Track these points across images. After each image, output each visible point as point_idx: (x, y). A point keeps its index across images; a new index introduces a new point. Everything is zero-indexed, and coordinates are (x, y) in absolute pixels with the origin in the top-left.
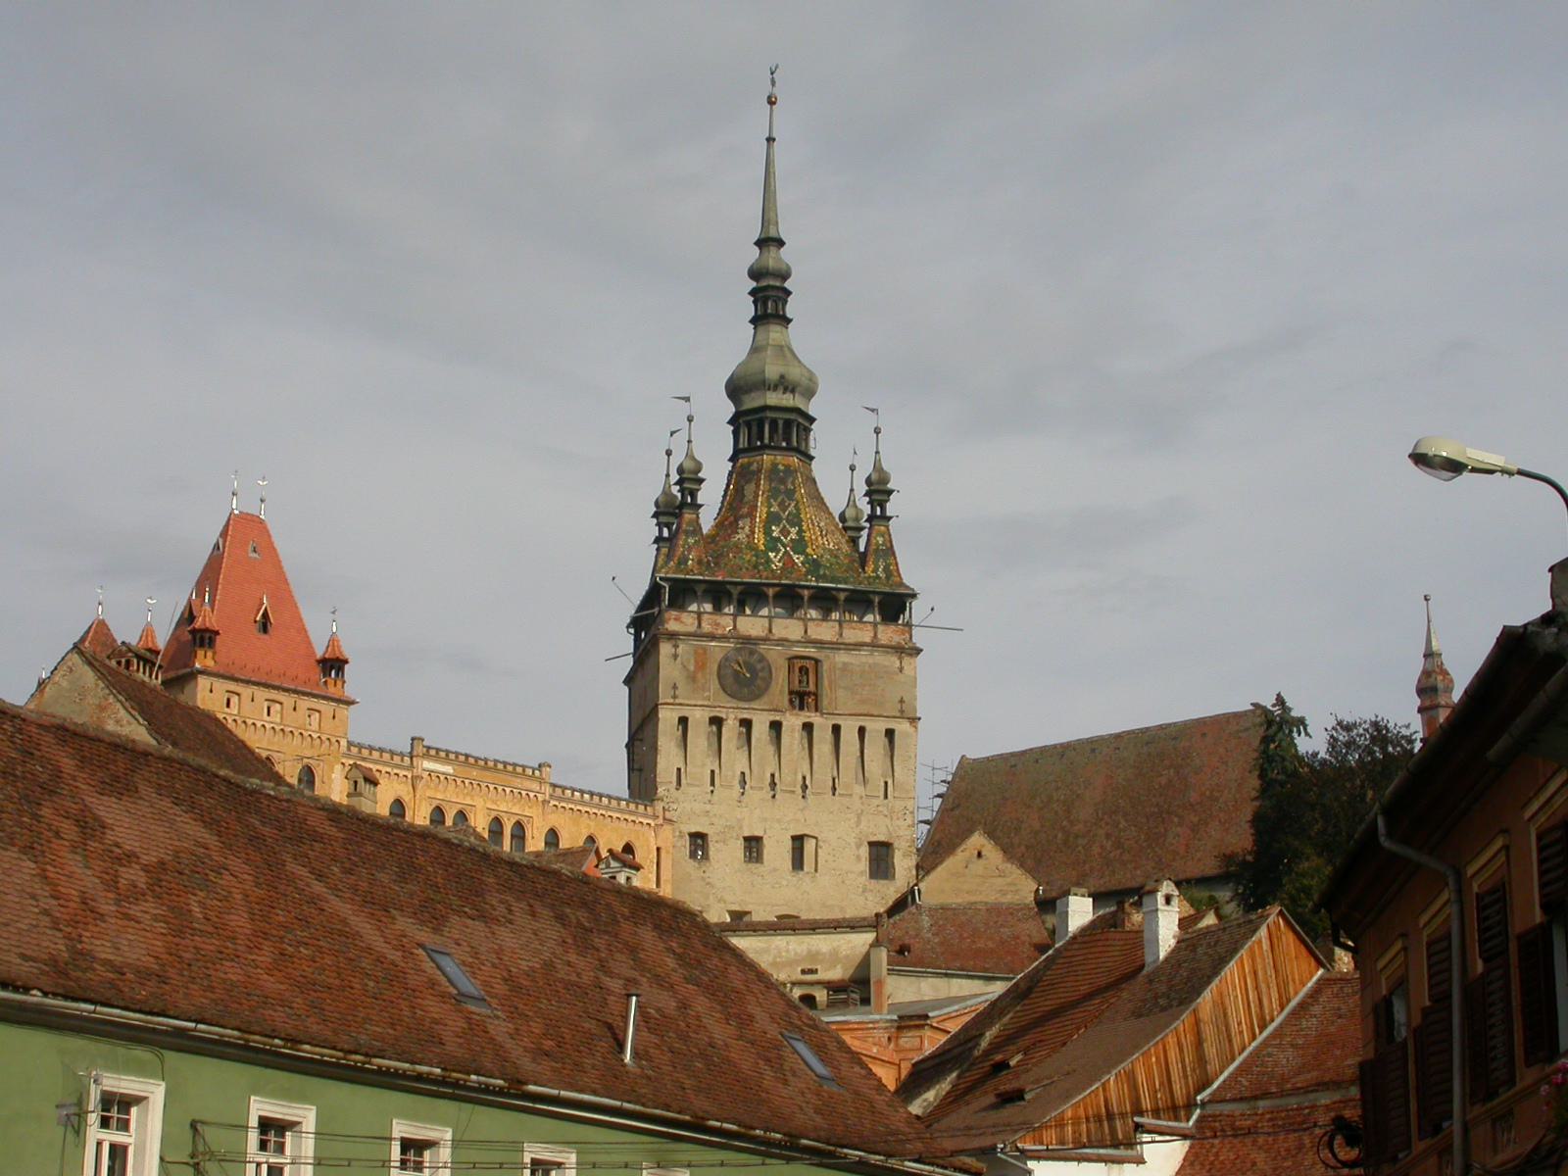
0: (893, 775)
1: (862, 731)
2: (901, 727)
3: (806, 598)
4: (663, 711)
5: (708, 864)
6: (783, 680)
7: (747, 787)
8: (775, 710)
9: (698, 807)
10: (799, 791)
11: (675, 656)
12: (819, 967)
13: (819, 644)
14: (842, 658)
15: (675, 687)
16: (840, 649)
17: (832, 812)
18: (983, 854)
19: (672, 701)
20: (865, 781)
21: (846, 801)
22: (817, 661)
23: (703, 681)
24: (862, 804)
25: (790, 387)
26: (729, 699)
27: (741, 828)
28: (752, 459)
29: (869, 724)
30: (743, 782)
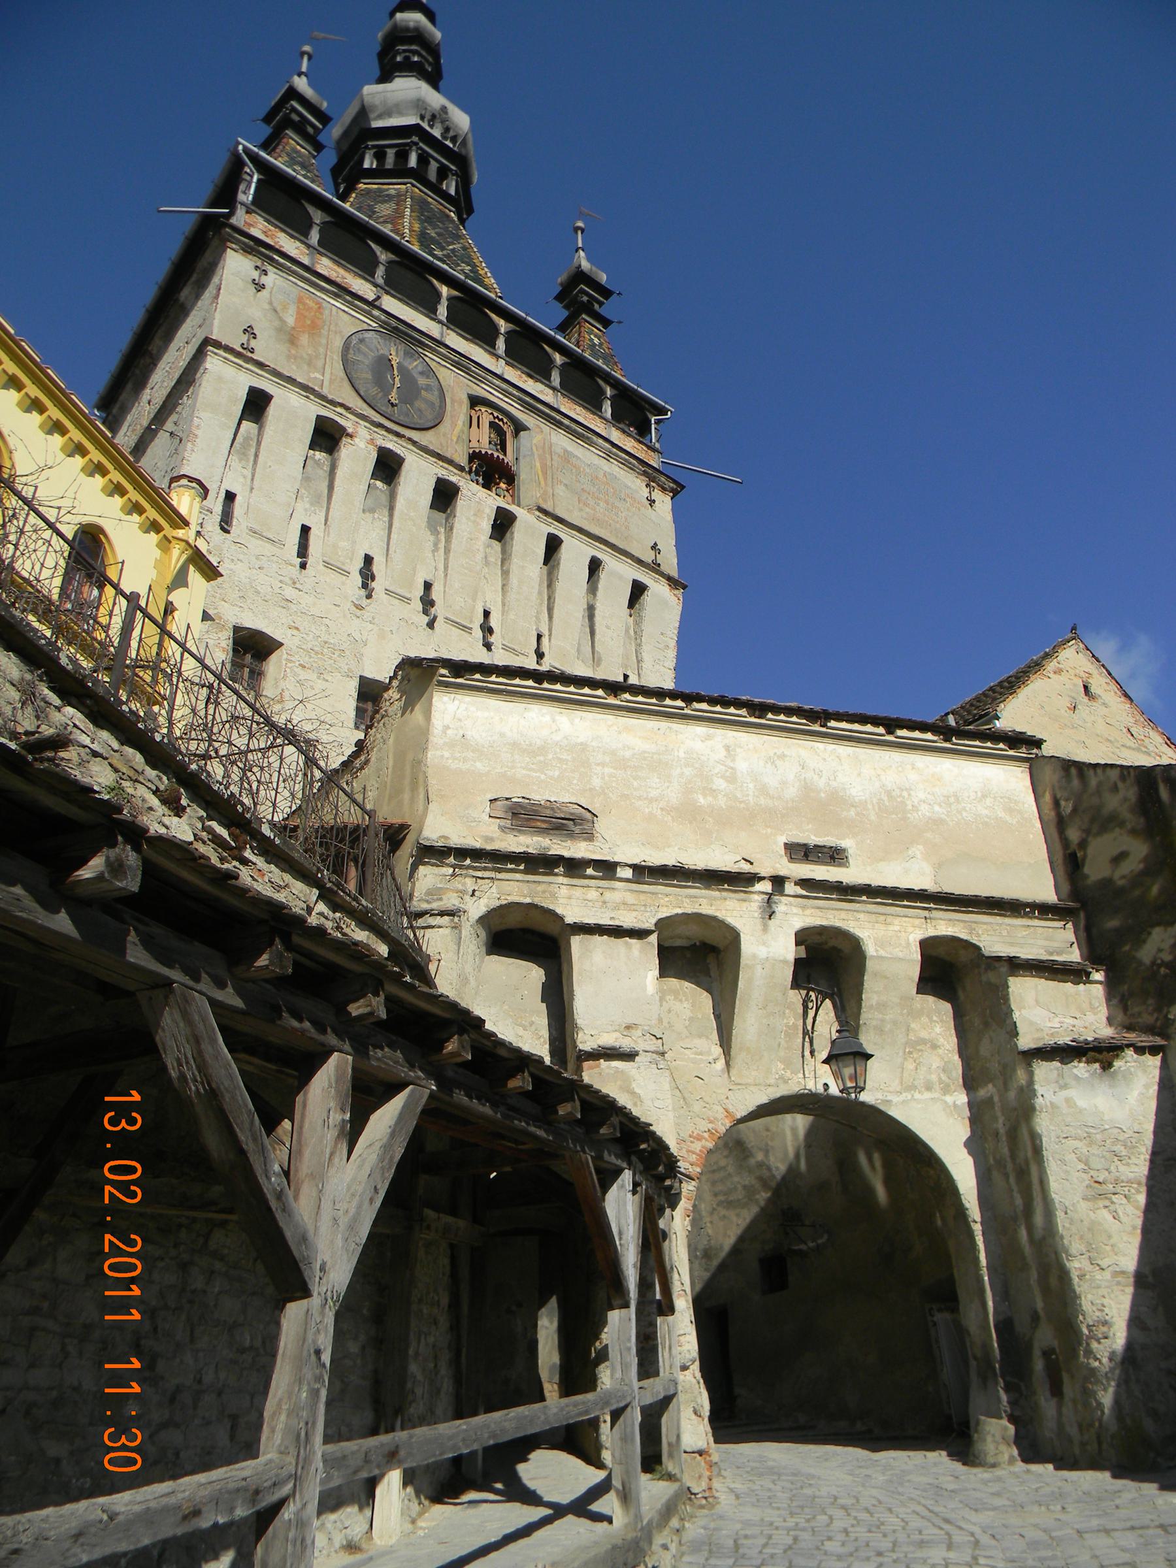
1: (595, 566)
2: (658, 589)
4: (214, 361)
6: (464, 425)
7: (377, 585)
8: (450, 462)
10: (479, 634)
11: (259, 287)
13: (531, 403)
14: (561, 440)
15: (249, 331)
16: (559, 424)
18: (1093, 689)
19: (241, 350)
22: (519, 428)
25: (451, 134)
27: (359, 658)
29: (610, 562)
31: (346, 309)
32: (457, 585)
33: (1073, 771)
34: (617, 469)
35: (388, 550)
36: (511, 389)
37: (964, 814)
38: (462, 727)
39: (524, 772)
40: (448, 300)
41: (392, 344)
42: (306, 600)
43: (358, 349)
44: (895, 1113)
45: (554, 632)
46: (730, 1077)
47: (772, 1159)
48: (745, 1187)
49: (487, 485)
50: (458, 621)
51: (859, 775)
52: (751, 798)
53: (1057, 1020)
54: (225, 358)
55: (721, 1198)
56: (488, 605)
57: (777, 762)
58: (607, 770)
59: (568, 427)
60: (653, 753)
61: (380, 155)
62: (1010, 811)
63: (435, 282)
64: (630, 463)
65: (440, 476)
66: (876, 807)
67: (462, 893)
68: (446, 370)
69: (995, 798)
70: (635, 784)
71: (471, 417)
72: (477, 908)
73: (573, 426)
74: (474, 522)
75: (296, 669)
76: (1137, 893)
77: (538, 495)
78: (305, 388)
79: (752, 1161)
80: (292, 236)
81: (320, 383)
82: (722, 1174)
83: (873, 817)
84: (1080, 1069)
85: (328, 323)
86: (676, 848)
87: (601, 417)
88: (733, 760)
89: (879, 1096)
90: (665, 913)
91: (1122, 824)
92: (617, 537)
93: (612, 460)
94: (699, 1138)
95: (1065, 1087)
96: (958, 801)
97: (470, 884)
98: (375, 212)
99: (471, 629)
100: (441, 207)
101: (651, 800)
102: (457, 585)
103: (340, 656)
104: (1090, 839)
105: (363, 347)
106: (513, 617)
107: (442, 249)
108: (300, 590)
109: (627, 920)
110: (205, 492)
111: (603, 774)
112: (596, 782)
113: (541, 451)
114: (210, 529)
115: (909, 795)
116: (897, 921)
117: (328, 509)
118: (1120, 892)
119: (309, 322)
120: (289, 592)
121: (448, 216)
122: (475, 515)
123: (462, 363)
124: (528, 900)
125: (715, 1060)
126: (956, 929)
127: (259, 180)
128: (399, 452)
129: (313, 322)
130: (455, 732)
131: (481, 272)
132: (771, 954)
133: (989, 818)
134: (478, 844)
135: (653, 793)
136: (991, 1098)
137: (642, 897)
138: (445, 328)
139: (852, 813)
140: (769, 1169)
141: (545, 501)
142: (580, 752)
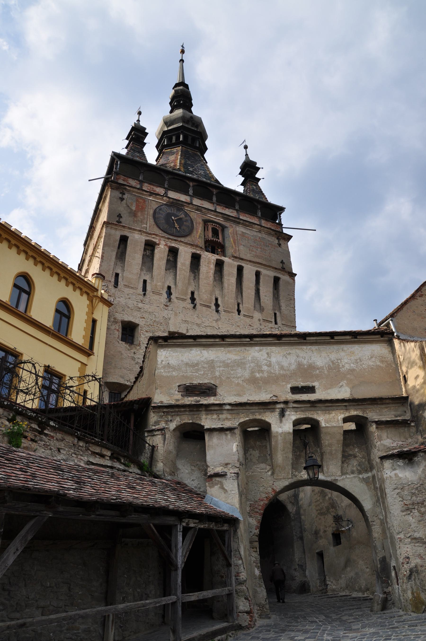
0: (280, 309)
2: (284, 278)
3: (215, 193)
5: (138, 348)
6: (201, 231)
7: (172, 296)
8: (197, 246)
9: (131, 303)
10: (214, 307)
11: (122, 199)
12: (316, 384)
13: (227, 218)
14: (240, 229)
15: (120, 216)
16: (239, 223)
17: (238, 326)
19: (117, 223)
20: (261, 310)
21: (248, 320)
22: (223, 228)
23: (141, 218)
24: (261, 324)
26: (161, 232)
27: (167, 324)
28: (173, 149)
29: (264, 272)
30: (169, 293)
31: (154, 200)
32: (203, 291)
33: (402, 344)
34: (264, 235)
35: (176, 283)
36: (218, 215)
37: (363, 366)
38: (168, 360)
39: (191, 374)
40: (192, 187)
41: (172, 208)
42: (147, 307)
43: (159, 213)
44: (340, 484)
45: (244, 302)
46: (274, 477)
47: (333, 497)
48: (325, 507)
49: (213, 252)
50: (205, 304)
51: (320, 356)
52: (277, 372)
53: (396, 443)
54: (111, 227)
55: (319, 512)
56: (217, 296)
57: (288, 356)
58: (221, 369)
59: (243, 223)
60: (239, 360)
61: (170, 139)
62: (382, 361)
63: (187, 182)
64: (269, 232)
65: (193, 252)
66: (327, 368)
67: (167, 422)
68: (193, 213)
69: (376, 357)
70: (232, 372)
71: (204, 227)
72: (173, 426)
73: (244, 222)
74: (208, 266)
75: (144, 333)
76: (422, 391)
77: (233, 251)
78: (140, 231)
79: (327, 498)
80: (133, 179)
81: (146, 228)
82: (318, 503)
83: (326, 372)
84: (400, 463)
85: (147, 206)
86: (248, 395)
87: (256, 217)
88: (270, 358)
89: (333, 478)
90: (242, 420)
91: (416, 364)
92: (266, 261)
93: (262, 232)
94: (262, 500)
95: (395, 469)
96: (361, 361)
97: (170, 418)
98: (168, 159)
99: (210, 306)
100: (193, 151)
101: (238, 378)
102: (203, 291)
103: (160, 325)
104: (408, 370)
105: (161, 212)
106: (227, 299)
107: (193, 167)
108: (144, 304)
109: (228, 424)
110: (104, 277)
111: (220, 370)
112: (217, 374)
113: (232, 235)
114: (110, 288)
115: (341, 361)
116: (333, 412)
117: (152, 272)
118: (418, 391)
119: (140, 207)
120: (140, 305)
121: (196, 154)
122: (208, 264)
123: (199, 209)
124: (191, 421)
125: (268, 471)
126: (358, 412)
127: (120, 163)
128: (176, 246)
129: (142, 207)
130: (165, 362)
131: (208, 172)
132: (283, 431)
133: (373, 365)
134: (173, 402)
135: (239, 375)
136: (375, 474)
137: (233, 415)
138: (192, 198)
139: (318, 372)
140: (333, 500)
141: (235, 253)
142: (211, 364)
